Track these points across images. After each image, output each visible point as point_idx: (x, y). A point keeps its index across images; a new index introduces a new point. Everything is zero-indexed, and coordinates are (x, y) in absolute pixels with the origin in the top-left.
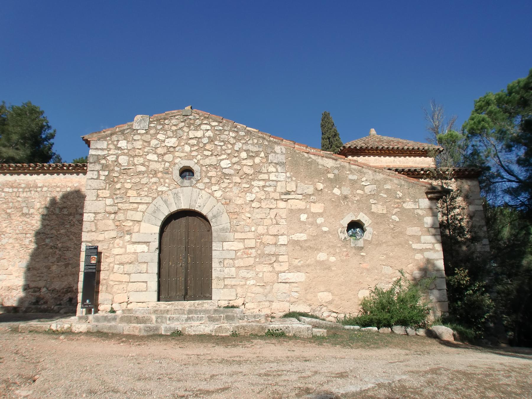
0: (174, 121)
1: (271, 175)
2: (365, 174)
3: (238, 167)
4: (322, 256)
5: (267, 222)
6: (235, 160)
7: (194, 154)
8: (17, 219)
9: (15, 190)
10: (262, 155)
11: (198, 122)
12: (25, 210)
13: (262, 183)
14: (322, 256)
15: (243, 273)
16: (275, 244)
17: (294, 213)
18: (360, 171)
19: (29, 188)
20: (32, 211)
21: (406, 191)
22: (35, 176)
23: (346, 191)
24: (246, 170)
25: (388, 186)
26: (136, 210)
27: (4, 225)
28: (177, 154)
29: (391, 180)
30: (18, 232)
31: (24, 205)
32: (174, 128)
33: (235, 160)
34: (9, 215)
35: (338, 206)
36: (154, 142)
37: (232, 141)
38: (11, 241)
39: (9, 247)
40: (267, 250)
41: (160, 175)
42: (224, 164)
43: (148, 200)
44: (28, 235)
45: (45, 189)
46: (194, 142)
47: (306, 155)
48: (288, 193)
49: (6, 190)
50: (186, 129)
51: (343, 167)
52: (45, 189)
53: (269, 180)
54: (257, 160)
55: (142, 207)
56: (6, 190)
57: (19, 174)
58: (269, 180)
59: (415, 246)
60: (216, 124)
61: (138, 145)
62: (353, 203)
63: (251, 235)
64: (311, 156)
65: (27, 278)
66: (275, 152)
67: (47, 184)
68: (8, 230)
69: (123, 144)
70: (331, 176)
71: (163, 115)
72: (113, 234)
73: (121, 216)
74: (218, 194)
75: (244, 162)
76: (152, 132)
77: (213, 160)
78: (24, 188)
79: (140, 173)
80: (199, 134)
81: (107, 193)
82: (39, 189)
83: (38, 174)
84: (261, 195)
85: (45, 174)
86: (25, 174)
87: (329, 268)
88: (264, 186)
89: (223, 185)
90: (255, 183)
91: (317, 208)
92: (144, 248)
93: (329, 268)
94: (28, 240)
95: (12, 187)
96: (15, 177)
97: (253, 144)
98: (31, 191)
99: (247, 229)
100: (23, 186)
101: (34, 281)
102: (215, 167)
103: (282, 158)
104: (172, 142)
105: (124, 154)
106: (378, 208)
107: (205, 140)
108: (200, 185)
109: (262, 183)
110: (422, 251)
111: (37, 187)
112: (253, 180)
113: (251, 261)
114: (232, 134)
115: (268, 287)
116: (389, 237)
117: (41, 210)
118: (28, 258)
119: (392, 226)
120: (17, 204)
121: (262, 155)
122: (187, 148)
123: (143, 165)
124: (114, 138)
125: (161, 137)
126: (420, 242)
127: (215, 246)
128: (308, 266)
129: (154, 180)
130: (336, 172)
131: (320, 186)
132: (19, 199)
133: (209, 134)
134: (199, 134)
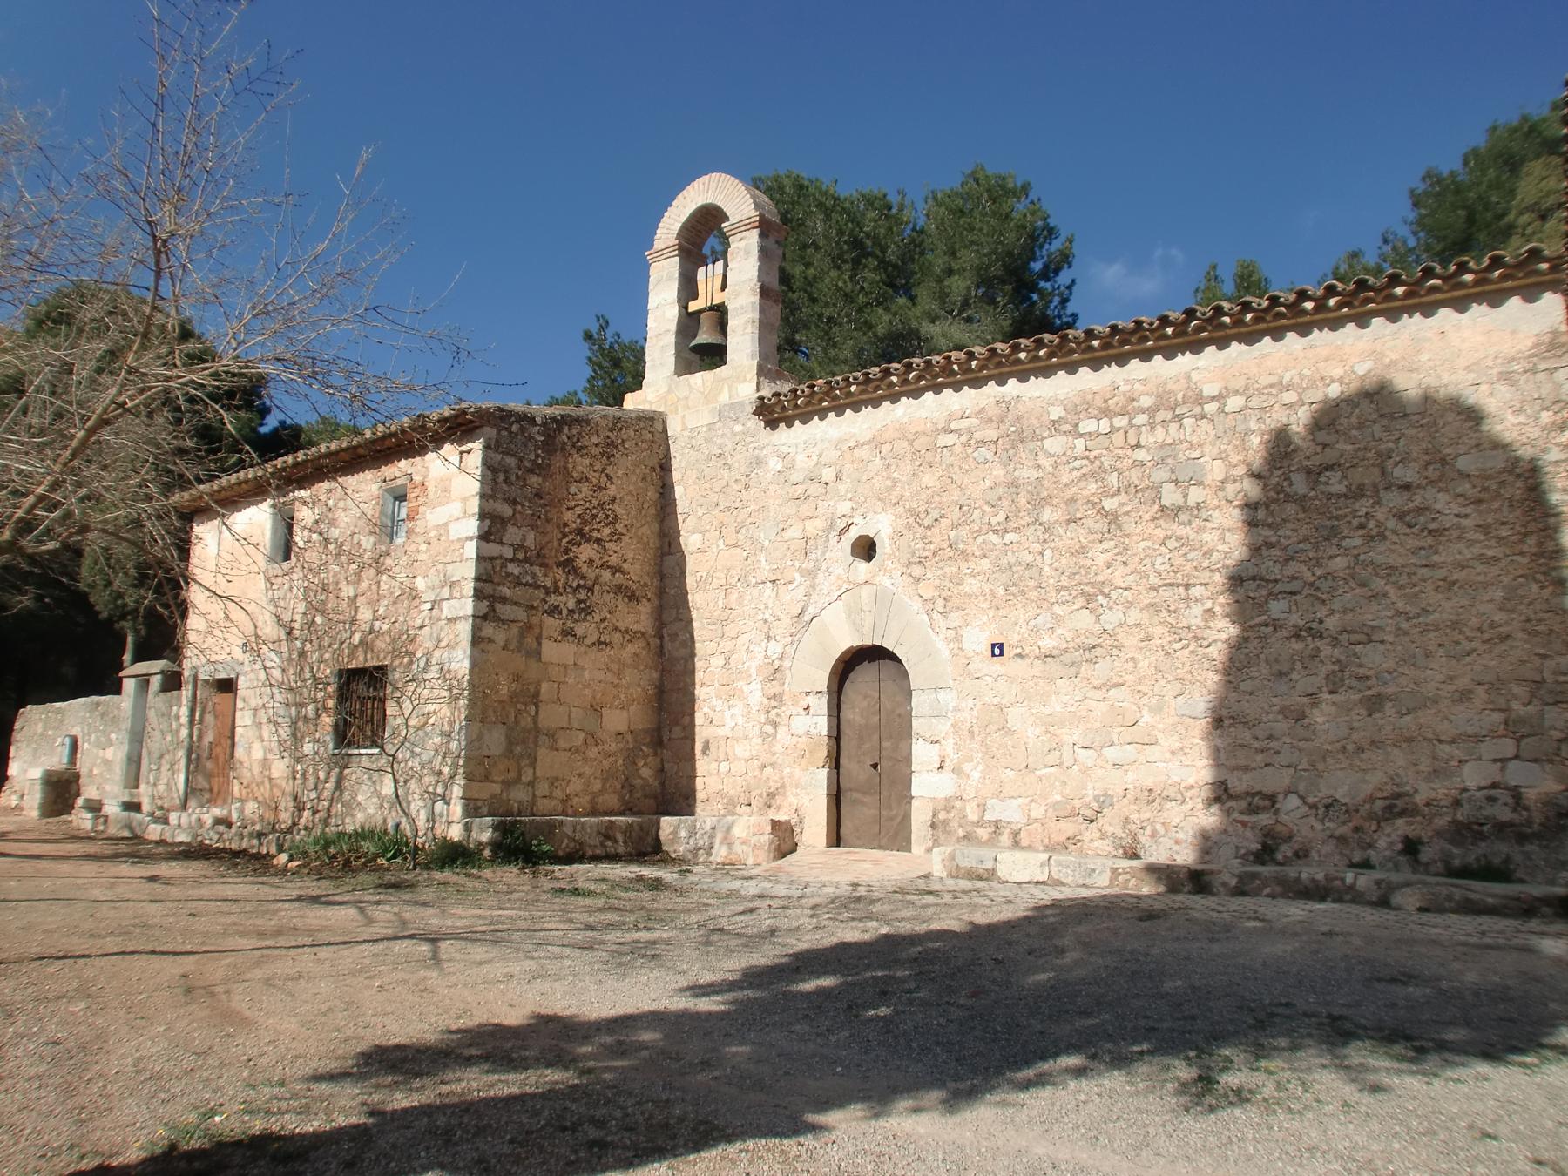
8: (1143, 532)
9: (1121, 422)
12: (1170, 496)
19: (1168, 407)
20: (1195, 495)
22: (1185, 360)
27: (1101, 559)
30: (1154, 580)
31: (1161, 474)
34: (1113, 518)
38: (1134, 616)
39: (1131, 641)
44: (1196, 591)
45: (1234, 403)
49: (1088, 426)
52: (1234, 403)
56: (1088, 426)
57: (1122, 360)
65: (1219, 758)
67: (1239, 383)
68: (1119, 576)
78: (1152, 411)
82: (1211, 408)
83: (1196, 347)
85: (1222, 344)
86: (1146, 356)
94: (1197, 610)
95: (1106, 413)
96: (1111, 372)
98: (1178, 418)
100: (1146, 402)
101: (1246, 769)
111: (1200, 400)
117: (1231, 489)
118: (1213, 679)
120: (1134, 476)
132: (1141, 455)
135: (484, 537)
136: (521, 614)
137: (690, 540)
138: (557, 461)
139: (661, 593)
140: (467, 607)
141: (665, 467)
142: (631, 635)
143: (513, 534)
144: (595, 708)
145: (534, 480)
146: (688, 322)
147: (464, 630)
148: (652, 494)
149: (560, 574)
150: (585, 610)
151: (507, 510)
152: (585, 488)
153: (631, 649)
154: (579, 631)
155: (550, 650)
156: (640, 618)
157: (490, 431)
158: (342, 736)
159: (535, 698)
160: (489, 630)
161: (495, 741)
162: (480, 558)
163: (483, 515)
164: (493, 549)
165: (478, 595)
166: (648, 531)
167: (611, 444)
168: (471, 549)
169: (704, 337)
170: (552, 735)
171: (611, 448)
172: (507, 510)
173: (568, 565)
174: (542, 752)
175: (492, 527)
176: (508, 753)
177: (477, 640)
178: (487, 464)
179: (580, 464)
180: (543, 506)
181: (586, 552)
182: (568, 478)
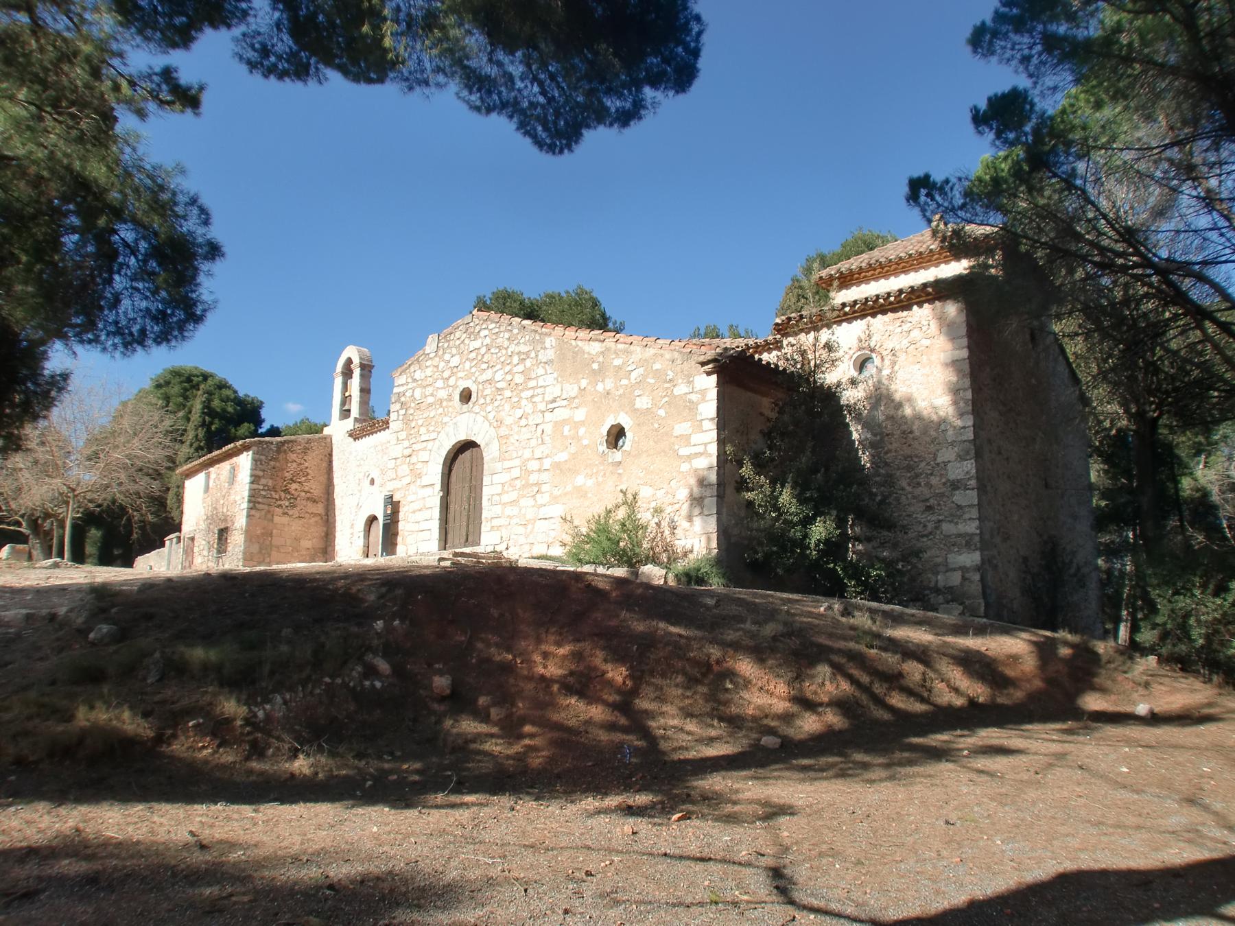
0: (458, 334)
1: (540, 379)
2: (631, 353)
3: (509, 377)
4: (580, 480)
5: (533, 442)
6: (508, 368)
7: (474, 370)
10: (533, 355)
11: (478, 328)
13: (530, 393)
14: (580, 480)
15: (509, 511)
16: (539, 470)
17: (558, 425)
18: (627, 352)
21: (678, 369)
23: (609, 384)
24: (519, 379)
25: (657, 366)
26: (424, 449)
28: (460, 375)
29: (662, 355)
32: (458, 342)
33: (508, 368)
35: (599, 408)
36: (442, 364)
37: (506, 343)
40: (533, 478)
41: (444, 404)
42: (498, 377)
43: (433, 435)
46: (473, 355)
47: (573, 342)
48: (554, 401)
50: (467, 341)
51: (608, 349)
53: (537, 387)
54: (528, 363)
55: (430, 444)
58: (537, 387)
59: (684, 451)
60: (493, 325)
61: (429, 372)
62: (614, 400)
63: (517, 462)
64: (579, 343)
66: (545, 348)
69: (418, 375)
70: (595, 366)
71: (449, 330)
72: (408, 479)
73: (414, 459)
74: (491, 416)
75: (515, 370)
76: (441, 352)
77: (488, 375)
79: (430, 405)
80: (477, 344)
81: (403, 435)
84: (529, 409)
87: (585, 496)
88: (532, 397)
89: (496, 404)
90: (524, 395)
91: (580, 415)
92: (429, 490)
93: (585, 496)
97: (525, 344)
99: (515, 455)
102: (489, 381)
103: (550, 354)
104: (455, 361)
105: (419, 386)
106: (643, 403)
107: (483, 350)
108: (477, 409)
109: (530, 393)
110: (689, 458)
112: (522, 391)
113: (513, 495)
114: (507, 335)
115: (530, 527)
116: (651, 443)
119: (656, 426)
121: (533, 355)
122: (467, 365)
123: (432, 395)
124: (412, 369)
125: (447, 357)
126: (688, 444)
127: (486, 480)
128: (566, 494)
129: (441, 410)
130: (601, 359)
131: (584, 383)
133: (488, 341)
134: (477, 344)
135: (252, 483)
136: (266, 507)
137: (336, 481)
138: (282, 456)
139: (328, 500)
140: (245, 505)
141: (331, 455)
142: (315, 515)
143: (263, 481)
144: (297, 539)
145: (272, 463)
146: (343, 403)
147: (245, 512)
148: (325, 464)
149: (283, 494)
150: (293, 506)
151: (261, 474)
152: (294, 465)
153: (314, 519)
154: (290, 513)
155: (277, 519)
156: (320, 509)
157: (255, 448)
158: (219, 552)
159: (271, 535)
160: (253, 512)
161: (255, 548)
162: (250, 490)
163: (252, 476)
164: (255, 486)
165: (249, 501)
166: (323, 479)
167: (306, 448)
168: (247, 487)
169: (346, 407)
170: (278, 547)
171: (305, 451)
172: (261, 474)
173: (287, 491)
174: (273, 553)
175: (255, 479)
176: (260, 552)
177: (249, 516)
178: (255, 460)
179: (292, 456)
180: (276, 472)
181: (294, 486)
182: (287, 461)
